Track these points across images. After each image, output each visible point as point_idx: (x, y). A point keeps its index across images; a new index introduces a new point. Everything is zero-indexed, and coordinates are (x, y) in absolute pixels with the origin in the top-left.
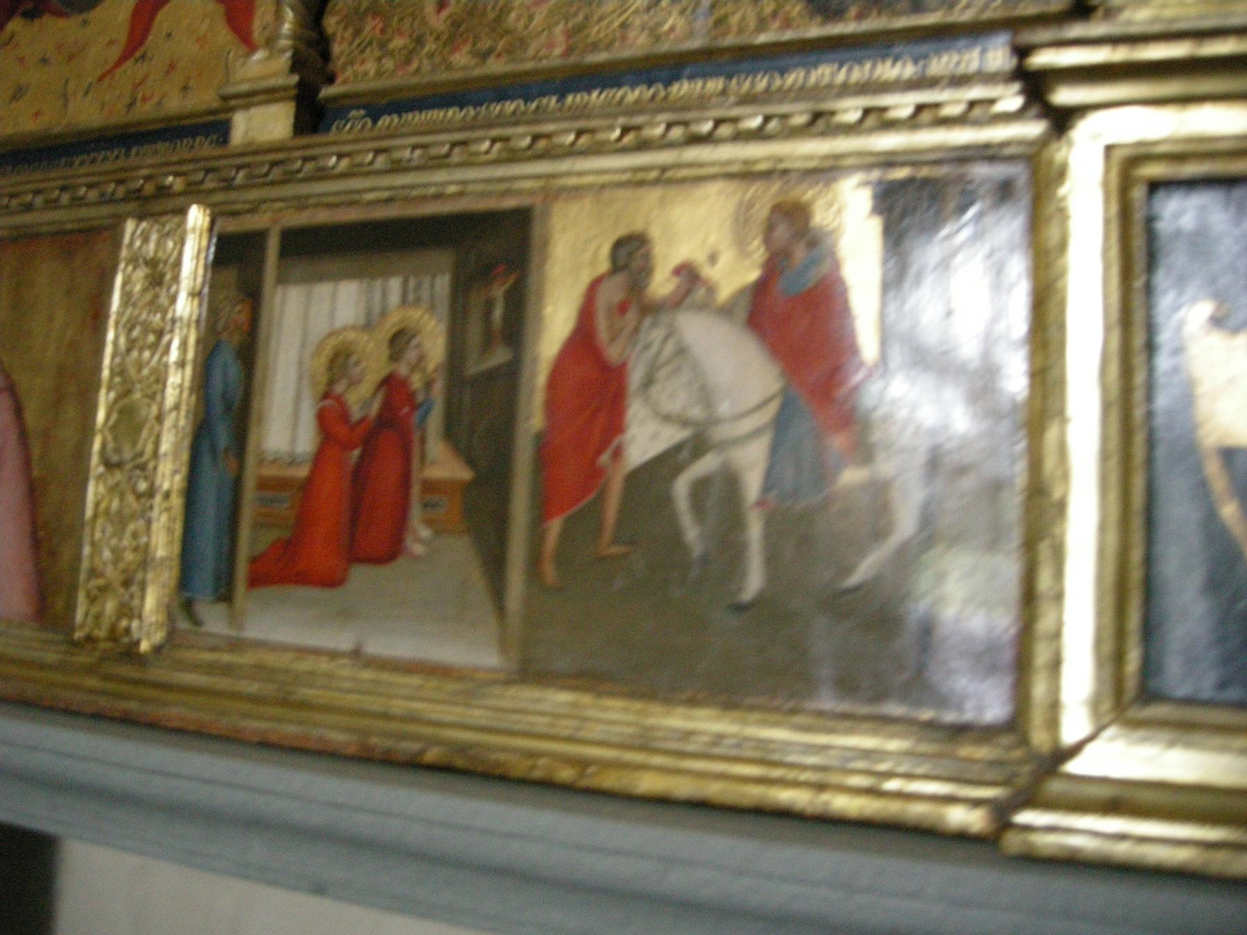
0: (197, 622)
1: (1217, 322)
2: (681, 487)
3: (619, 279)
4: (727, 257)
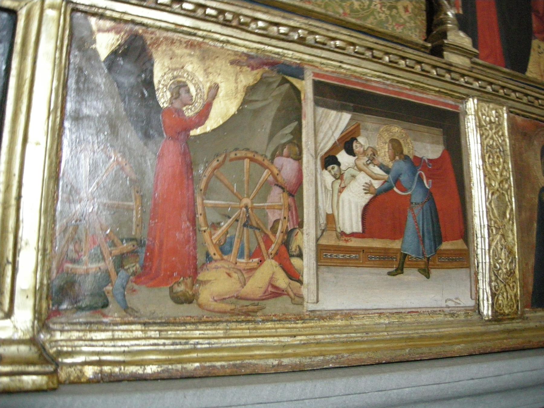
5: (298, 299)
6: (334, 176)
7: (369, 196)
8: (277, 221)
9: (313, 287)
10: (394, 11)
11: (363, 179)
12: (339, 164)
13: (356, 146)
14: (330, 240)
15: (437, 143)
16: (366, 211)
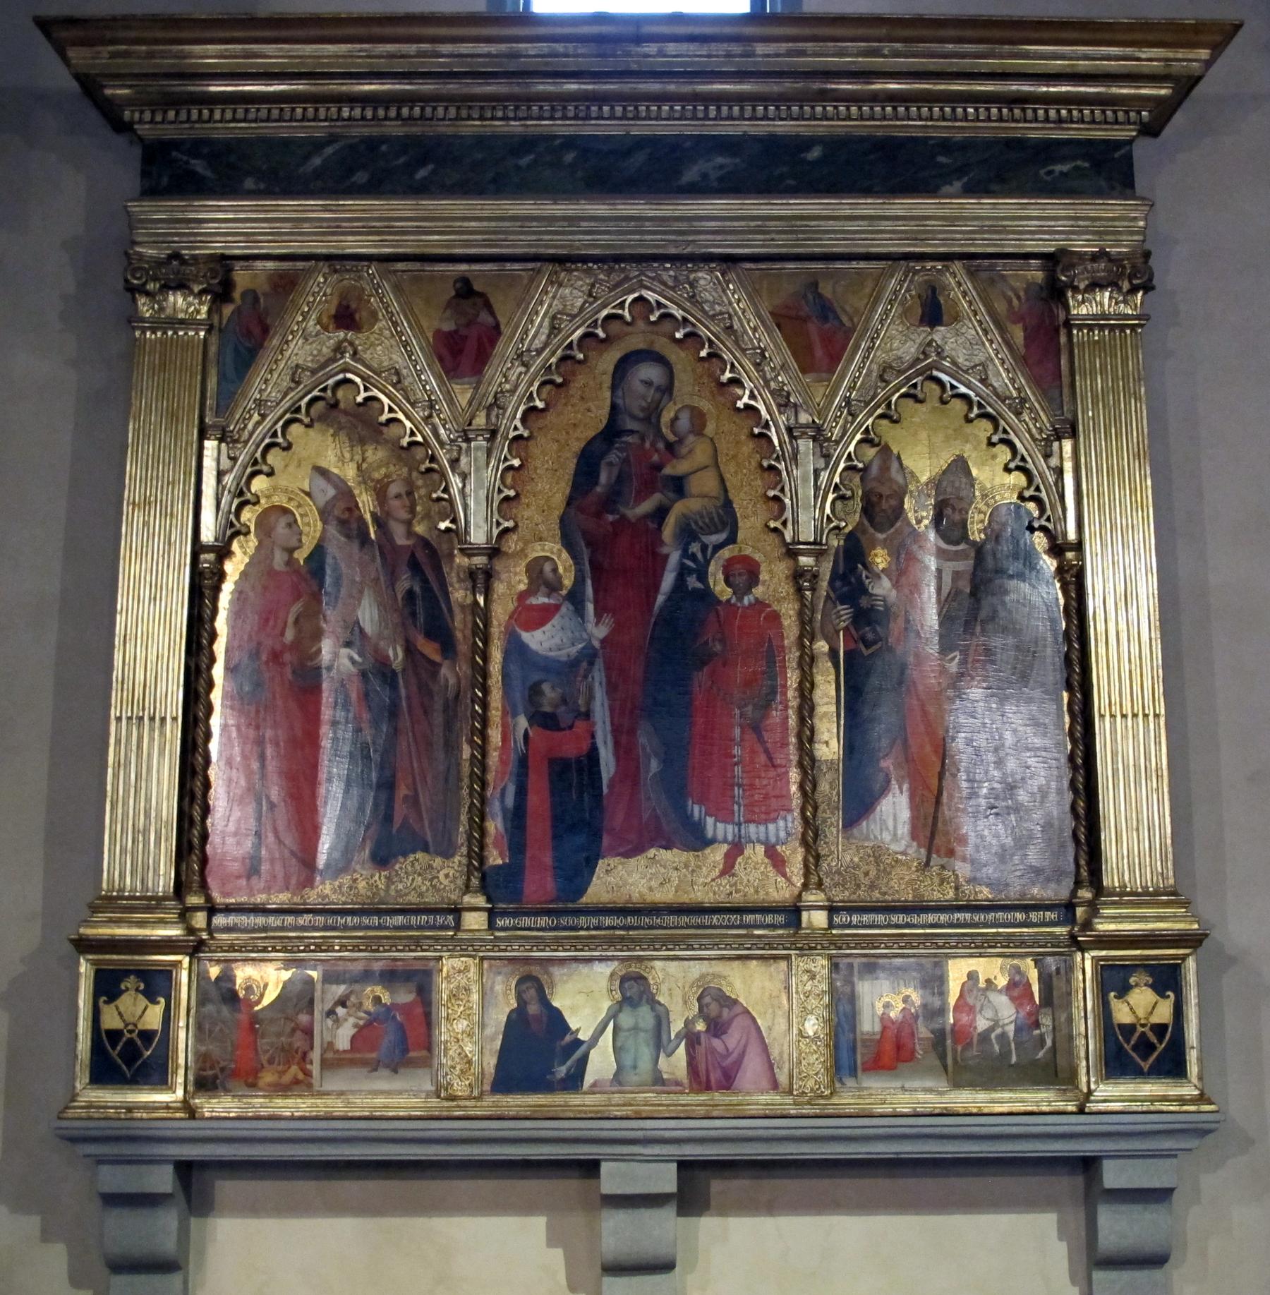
0: (843, 1084)
1: (1115, 997)
2: (993, 1036)
3: (970, 982)
4: (999, 976)
5: (310, 1086)
6: (334, 1021)
7: (356, 1030)
8: (298, 1048)
9: (319, 1079)
10: (436, 880)
11: (352, 1020)
12: (337, 1015)
13: (348, 1003)
14: (330, 1055)
15: (410, 992)
16: (353, 1039)
